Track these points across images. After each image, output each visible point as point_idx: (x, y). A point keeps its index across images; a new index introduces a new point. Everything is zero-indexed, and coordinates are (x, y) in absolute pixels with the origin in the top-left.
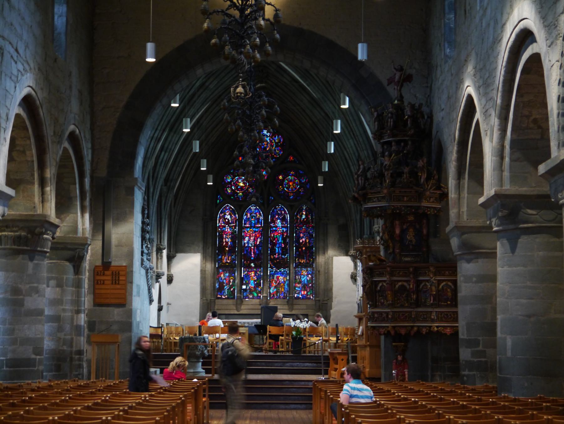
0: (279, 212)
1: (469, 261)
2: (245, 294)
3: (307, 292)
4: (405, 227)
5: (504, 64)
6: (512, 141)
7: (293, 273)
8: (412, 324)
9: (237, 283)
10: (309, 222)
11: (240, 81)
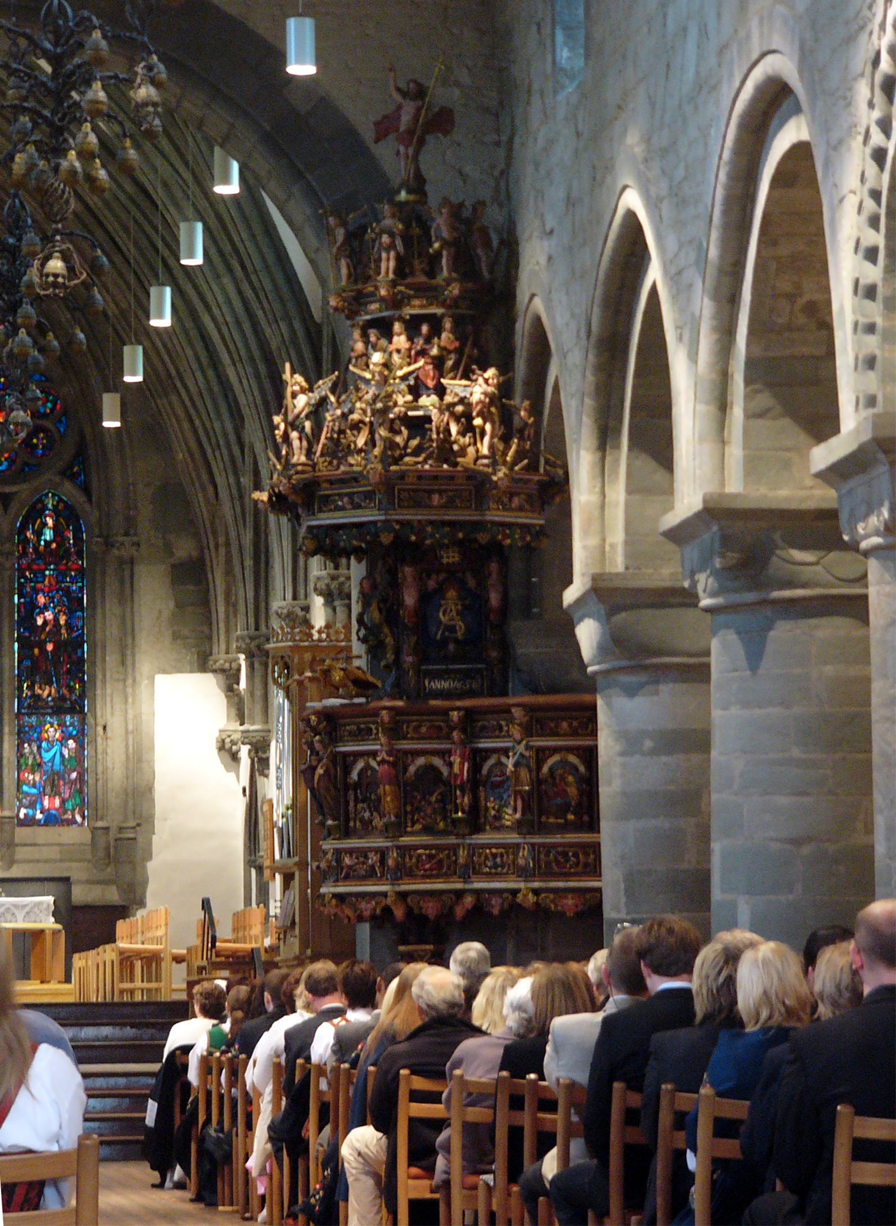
1: (631, 692)
3: (63, 802)
4: (432, 584)
5: (726, 155)
6: (751, 363)
8: (459, 886)
10: (67, 555)
11: (58, 241)
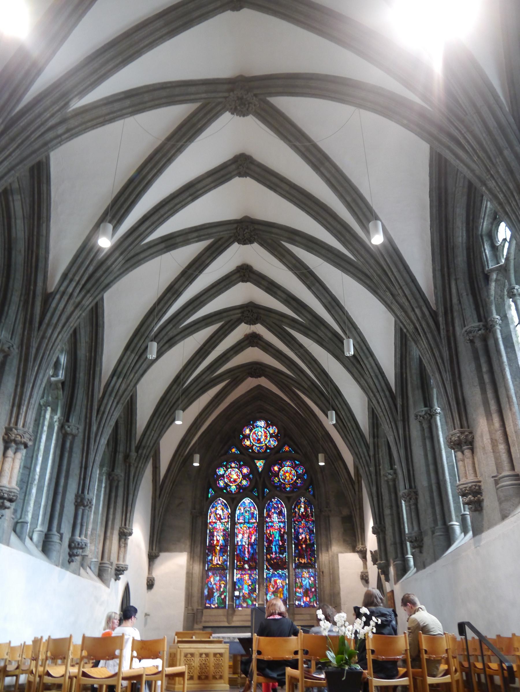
0: (275, 505)
2: (238, 602)
3: (310, 599)
7: (292, 575)
9: (229, 589)
10: (308, 516)
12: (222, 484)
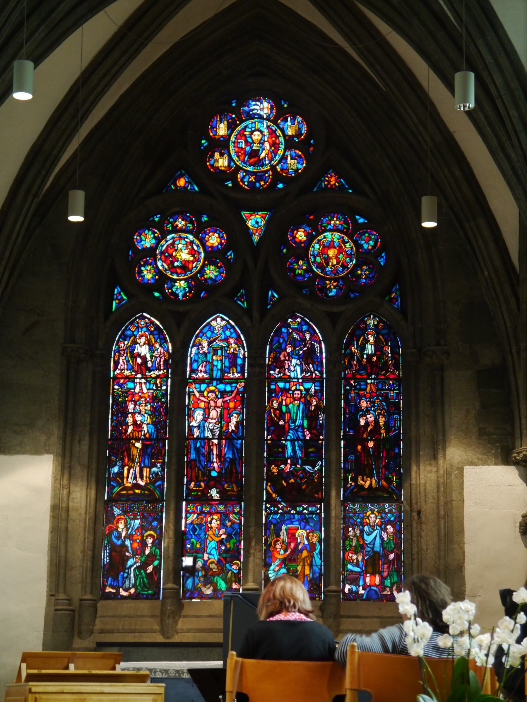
0: (295, 336)
2: (190, 582)
3: (382, 579)
7: (337, 517)
9: (166, 549)
12: (148, 274)
